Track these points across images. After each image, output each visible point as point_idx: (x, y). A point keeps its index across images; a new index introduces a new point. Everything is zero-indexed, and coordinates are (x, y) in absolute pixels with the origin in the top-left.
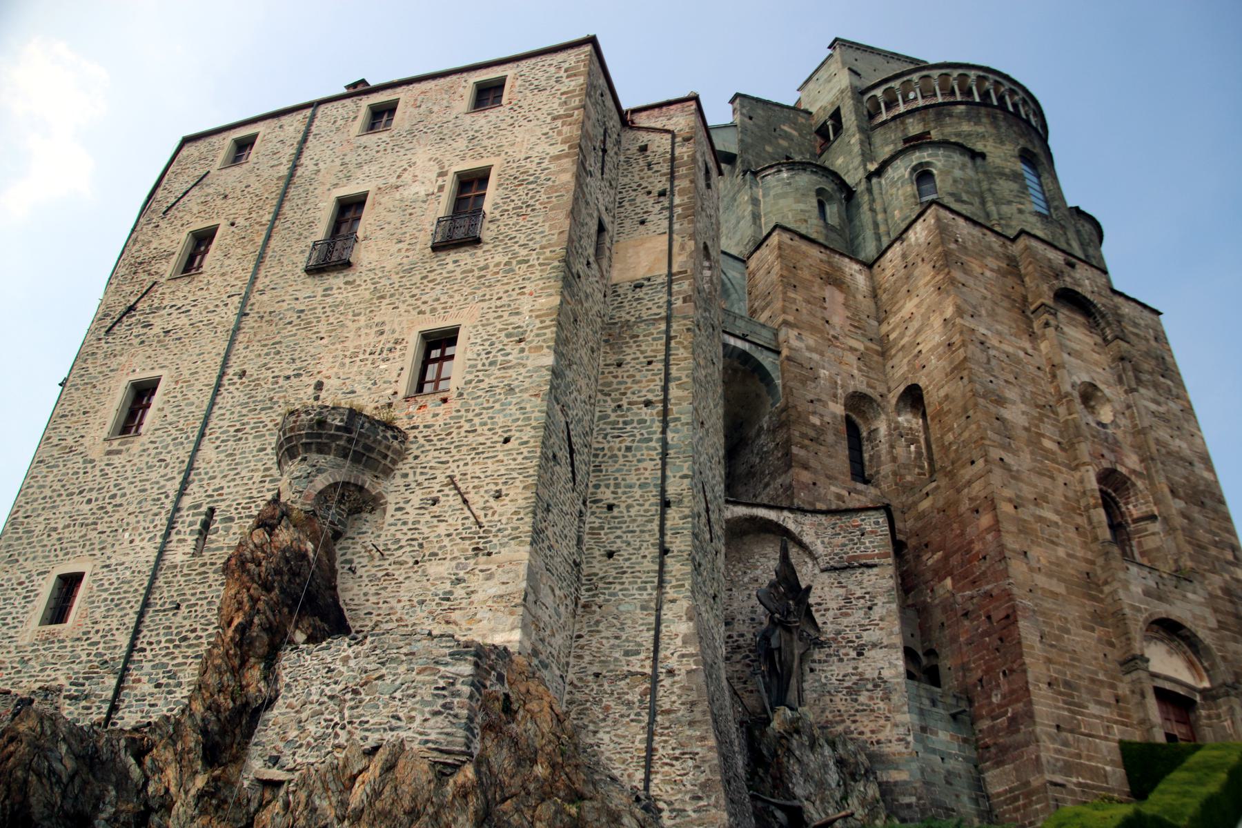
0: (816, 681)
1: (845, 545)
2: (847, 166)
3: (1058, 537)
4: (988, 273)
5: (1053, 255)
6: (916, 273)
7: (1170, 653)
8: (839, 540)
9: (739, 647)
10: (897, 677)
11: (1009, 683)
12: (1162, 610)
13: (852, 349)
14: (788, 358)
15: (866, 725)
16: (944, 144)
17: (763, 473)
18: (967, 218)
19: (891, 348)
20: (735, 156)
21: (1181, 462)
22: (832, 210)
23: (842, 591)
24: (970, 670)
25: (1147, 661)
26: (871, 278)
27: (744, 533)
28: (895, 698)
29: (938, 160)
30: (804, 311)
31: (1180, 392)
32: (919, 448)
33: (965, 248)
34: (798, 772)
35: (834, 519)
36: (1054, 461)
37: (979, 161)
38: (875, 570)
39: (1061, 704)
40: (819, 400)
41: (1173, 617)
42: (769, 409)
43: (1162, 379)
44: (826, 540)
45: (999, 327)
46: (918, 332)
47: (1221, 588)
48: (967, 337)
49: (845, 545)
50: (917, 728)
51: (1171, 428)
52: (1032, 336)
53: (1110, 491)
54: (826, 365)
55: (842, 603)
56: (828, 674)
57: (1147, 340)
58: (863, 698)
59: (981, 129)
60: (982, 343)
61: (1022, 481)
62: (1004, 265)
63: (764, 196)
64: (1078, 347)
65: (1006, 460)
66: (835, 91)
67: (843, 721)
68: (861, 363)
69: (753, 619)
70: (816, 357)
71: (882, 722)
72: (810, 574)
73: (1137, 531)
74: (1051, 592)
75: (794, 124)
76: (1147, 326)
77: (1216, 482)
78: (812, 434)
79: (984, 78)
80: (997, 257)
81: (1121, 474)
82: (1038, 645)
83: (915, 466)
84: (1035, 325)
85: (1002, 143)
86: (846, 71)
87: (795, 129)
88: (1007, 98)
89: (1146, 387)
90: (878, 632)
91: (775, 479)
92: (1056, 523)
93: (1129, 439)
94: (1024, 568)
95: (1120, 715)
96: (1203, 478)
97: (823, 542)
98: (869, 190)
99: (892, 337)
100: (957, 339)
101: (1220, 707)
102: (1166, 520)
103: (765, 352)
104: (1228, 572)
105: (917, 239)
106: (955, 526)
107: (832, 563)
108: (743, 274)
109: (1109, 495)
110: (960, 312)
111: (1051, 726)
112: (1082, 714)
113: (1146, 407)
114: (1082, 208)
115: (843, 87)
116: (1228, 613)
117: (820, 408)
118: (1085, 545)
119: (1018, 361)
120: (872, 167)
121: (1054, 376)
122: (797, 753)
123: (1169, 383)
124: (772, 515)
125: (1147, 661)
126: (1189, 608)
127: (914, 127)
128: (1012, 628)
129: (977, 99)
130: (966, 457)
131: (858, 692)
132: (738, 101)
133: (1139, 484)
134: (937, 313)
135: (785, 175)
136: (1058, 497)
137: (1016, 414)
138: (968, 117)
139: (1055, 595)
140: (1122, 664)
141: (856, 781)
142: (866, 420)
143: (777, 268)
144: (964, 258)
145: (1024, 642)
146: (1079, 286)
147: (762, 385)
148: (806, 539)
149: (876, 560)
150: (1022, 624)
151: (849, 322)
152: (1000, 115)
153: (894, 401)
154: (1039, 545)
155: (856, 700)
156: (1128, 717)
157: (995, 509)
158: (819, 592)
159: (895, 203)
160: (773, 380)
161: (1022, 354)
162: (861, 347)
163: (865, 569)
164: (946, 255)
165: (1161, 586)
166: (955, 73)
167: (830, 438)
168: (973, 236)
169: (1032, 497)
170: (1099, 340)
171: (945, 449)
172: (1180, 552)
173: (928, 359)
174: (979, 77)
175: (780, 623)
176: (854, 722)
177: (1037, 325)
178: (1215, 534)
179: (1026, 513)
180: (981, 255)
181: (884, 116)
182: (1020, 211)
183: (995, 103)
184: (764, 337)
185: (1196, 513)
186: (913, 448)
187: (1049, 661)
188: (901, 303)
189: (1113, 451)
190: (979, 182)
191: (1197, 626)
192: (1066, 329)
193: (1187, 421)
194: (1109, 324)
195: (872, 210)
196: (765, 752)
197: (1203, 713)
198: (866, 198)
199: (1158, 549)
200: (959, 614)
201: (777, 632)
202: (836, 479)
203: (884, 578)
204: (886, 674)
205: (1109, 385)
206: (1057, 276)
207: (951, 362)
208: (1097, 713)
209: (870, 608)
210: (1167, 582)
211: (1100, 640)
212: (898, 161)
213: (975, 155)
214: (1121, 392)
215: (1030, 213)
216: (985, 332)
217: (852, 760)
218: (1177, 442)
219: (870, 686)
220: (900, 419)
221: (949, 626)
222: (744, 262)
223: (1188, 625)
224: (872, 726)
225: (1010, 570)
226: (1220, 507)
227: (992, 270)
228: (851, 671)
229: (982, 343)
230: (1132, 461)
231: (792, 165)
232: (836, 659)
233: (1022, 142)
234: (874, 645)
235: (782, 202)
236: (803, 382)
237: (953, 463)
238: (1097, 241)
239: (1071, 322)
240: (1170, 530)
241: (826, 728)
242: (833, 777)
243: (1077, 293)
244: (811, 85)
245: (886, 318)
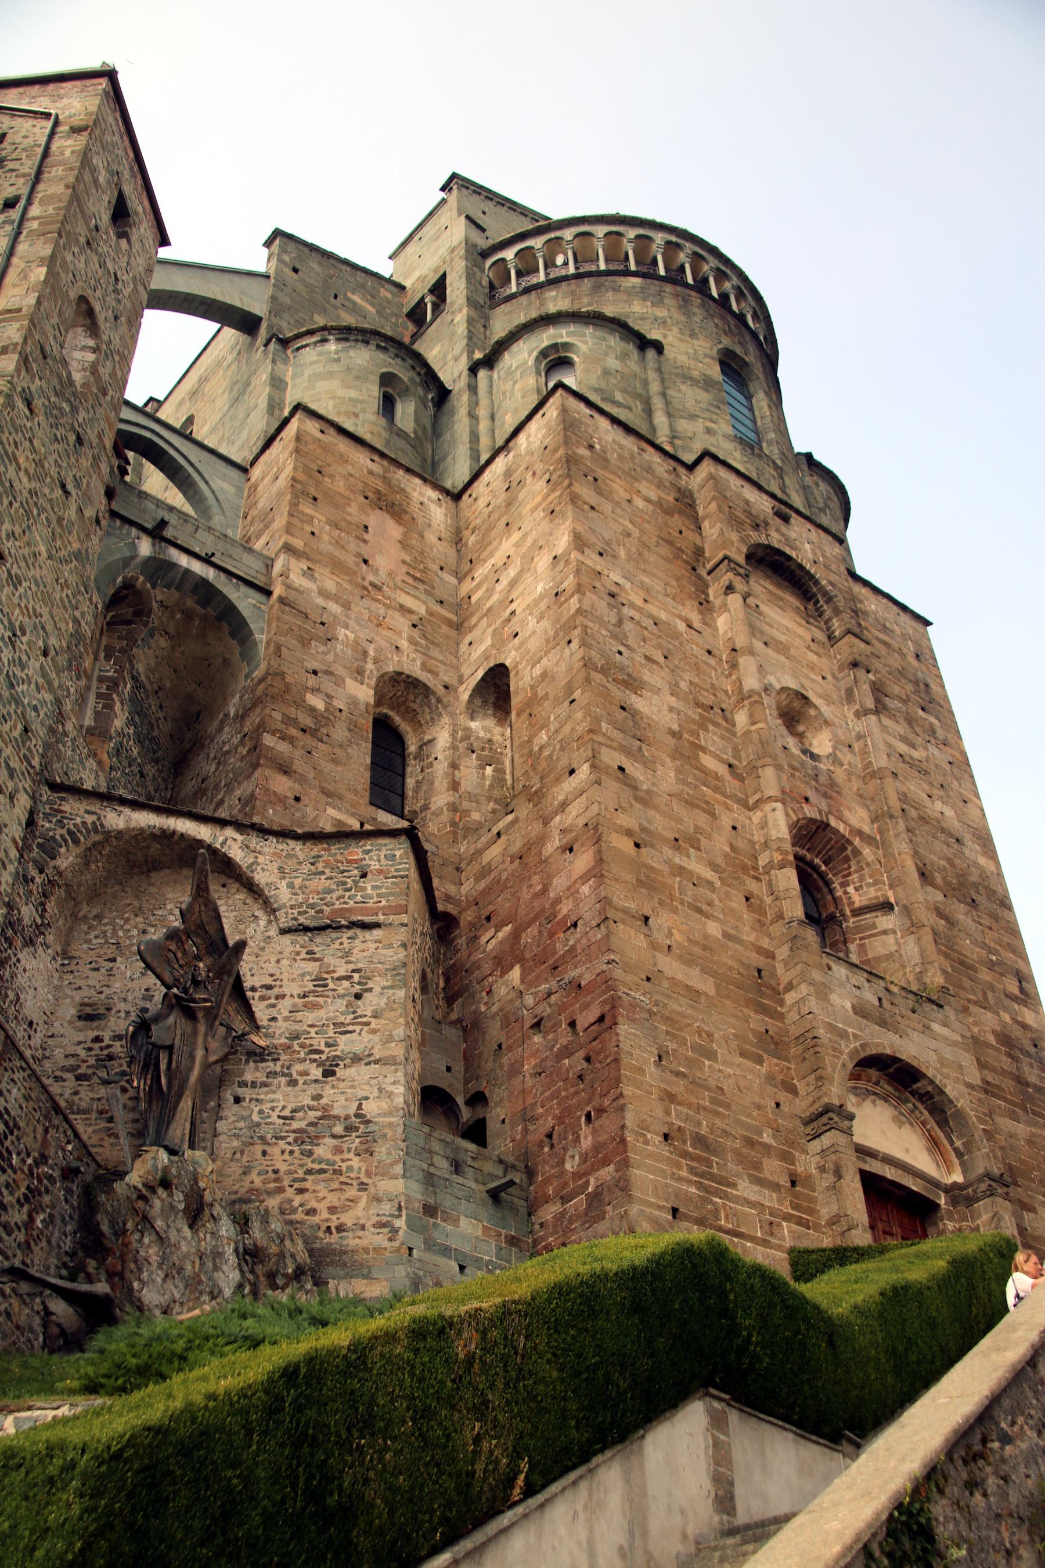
0: (243, 1118)
1: (330, 891)
2: (445, 355)
3: (710, 904)
4: (639, 503)
6: (521, 497)
7: (898, 1121)
8: (322, 883)
9: (110, 1058)
10: (390, 1114)
11: (595, 1132)
12: (886, 1042)
13: (403, 609)
14: (282, 600)
15: (322, 1197)
16: (596, 319)
17: (217, 787)
18: (615, 420)
19: (472, 614)
20: (259, 320)
21: (942, 837)
22: (406, 413)
23: (312, 967)
24: (534, 1119)
25: (851, 1117)
26: (457, 515)
27: (152, 866)
28: (382, 1150)
29: (584, 342)
30: (326, 537)
31: (949, 736)
32: (500, 771)
33: (606, 460)
34: (154, 1259)
35: (317, 849)
36: (716, 789)
37: (651, 354)
38: (377, 933)
39: (684, 1173)
40: (327, 672)
41: (904, 1057)
42: (242, 683)
43: (921, 712)
44: (298, 882)
45: (647, 580)
46: (513, 584)
47: (993, 1032)
48: (585, 580)
49: (330, 891)
50: (417, 1206)
51: (931, 784)
52: (704, 604)
53: (817, 861)
54: (352, 623)
55: (310, 986)
56: (266, 1107)
57: (903, 655)
58: (323, 1150)
59: (661, 313)
60: (612, 595)
61: (656, 808)
62: (671, 499)
63: (294, 376)
64: (783, 638)
65: (629, 770)
66: (443, 251)
67: (280, 1190)
68: (416, 633)
69: (145, 1010)
70: (334, 608)
71: (352, 1192)
72: (259, 936)
73: (859, 929)
74: (687, 986)
75: (372, 296)
76: (905, 636)
77: (1000, 874)
78: (308, 721)
79: (678, 245)
80: (660, 484)
81: (836, 831)
82: (651, 1069)
83: (490, 799)
84: (711, 592)
85: (693, 335)
86: (463, 218)
87: (372, 305)
88: (712, 280)
89: (892, 717)
90: (366, 1037)
91: (233, 791)
92: (710, 883)
93: (856, 784)
94: (641, 941)
95: (796, 1207)
96: (976, 865)
97: (291, 886)
98: (473, 389)
99: (474, 599)
100: (569, 583)
101: (980, 1216)
102: (907, 910)
103: (244, 589)
104: (1006, 1009)
105: (529, 443)
106: (536, 879)
107: (302, 920)
108: (240, 489)
109: (816, 868)
110: (579, 542)
111: (660, 1208)
112: (725, 1196)
113: (890, 746)
114: (817, 457)
115: (455, 243)
116: (1004, 1072)
117: (327, 684)
118: (761, 925)
119: (676, 635)
120: (478, 355)
121: (734, 666)
122: (159, 1223)
123: (933, 720)
124: (203, 832)
125: (851, 1117)
126: (931, 1046)
127: (556, 301)
128: (606, 1035)
129: (662, 272)
130: (563, 763)
131: (315, 1140)
132: (277, 242)
133: (867, 852)
134: (545, 551)
135: (332, 346)
136: (720, 843)
137: (658, 707)
138: (643, 295)
139: (694, 994)
140: (806, 1123)
141: (274, 1287)
142: (418, 726)
143: (289, 470)
144: (600, 473)
145: (625, 1059)
146: (792, 548)
147: (233, 643)
148: (261, 878)
149: (381, 918)
150: (623, 1028)
151: (405, 569)
152: (696, 298)
153: (465, 695)
154: (675, 910)
155: (310, 1153)
156: (811, 1211)
157: (598, 841)
158: (271, 968)
159: (508, 404)
160: (251, 633)
161: (682, 626)
162: (422, 610)
163: (358, 931)
164: (570, 461)
165: (886, 1004)
166: (632, 233)
167: (340, 732)
168: (621, 447)
169: (672, 836)
170: (821, 636)
171: (533, 757)
172: (925, 962)
173: (524, 622)
174: (669, 243)
175: (181, 1005)
176: (301, 1191)
177: (714, 592)
178: (990, 951)
179: (655, 858)
180: (632, 476)
181: (514, 288)
182: (709, 431)
183: (690, 280)
184: (248, 566)
185: (960, 912)
186: (489, 770)
187: (670, 1097)
188: (495, 543)
189: (825, 795)
190: (646, 383)
191: (947, 1077)
192: (763, 608)
193: (958, 780)
194: (837, 611)
195: (473, 416)
196: (105, 1228)
197: (950, 1225)
198: (465, 398)
199: (890, 957)
200: (527, 1025)
201: (171, 1019)
202: (340, 797)
203: (390, 946)
204: (370, 1108)
205: (829, 702)
206: (756, 527)
207: (557, 620)
208: (753, 1198)
209: (358, 996)
210: (899, 1000)
211: (770, 1078)
212: (521, 342)
213: (644, 343)
214: (850, 715)
215: (726, 436)
216: (621, 581)
217: (274, 1249)
218: (938, 806)
219: (339, 1129)
220: (474, 725)
221: (510, 1049)
222: (245, 470)
223: (930, 1073)
224: (333, 1199)
225: (613, 939)
226: (1002, 912)
227: (647, 500)
228: (307, 1101)
229: (612, 595)
230: (852, 818)
231: (346, 333)
232: (283, 1080)
233: (726, 342)
234: (356, 1059)
235: (322, 386)
236: (305, 642)
237: (542, 778)
238: (839, 513)
239: (774, 600)
240: (914, 927)
241: (248, 1201)
242: (229, 1276)
243: (789, 558)
244: (410, 249)
245: (471, 570)
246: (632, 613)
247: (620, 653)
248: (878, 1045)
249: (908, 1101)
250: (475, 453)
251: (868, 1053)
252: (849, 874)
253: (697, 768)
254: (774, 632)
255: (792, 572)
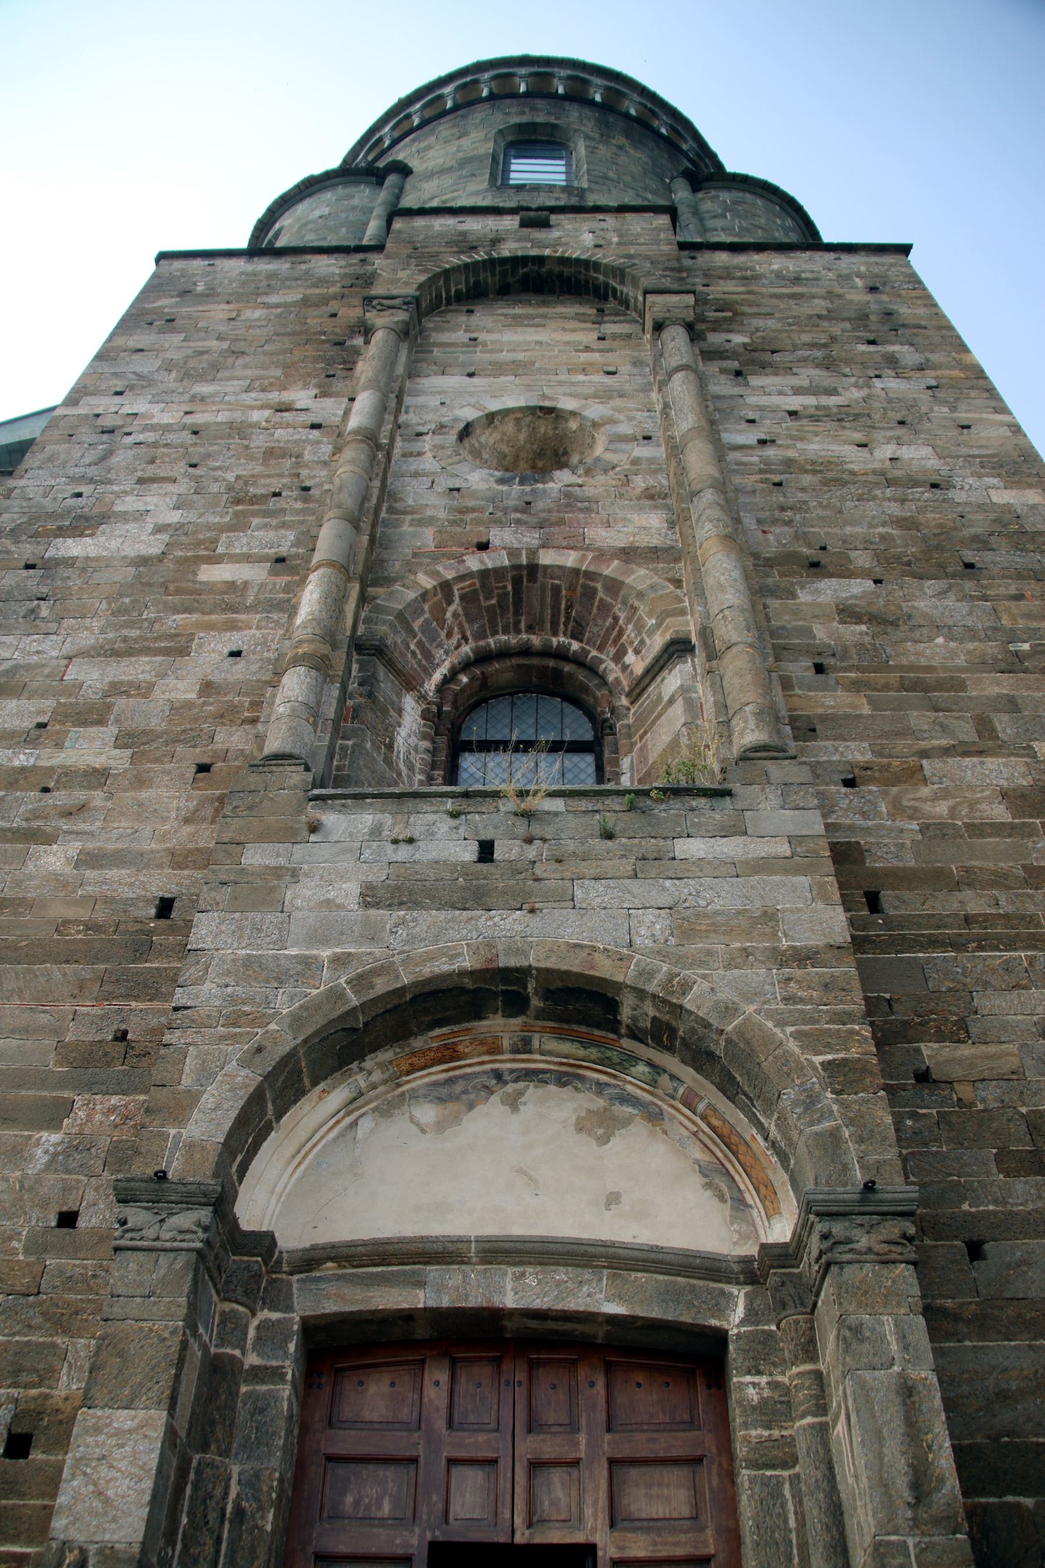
4: (258, 313)
5: (474, 225)
12: (448, 943)
37: (391, 179)
43: (863, 348)
64: (520, 356)
76: (844, 278)
109: (562, 654)
133: (639, 577)
233: (515, 120)
243: (540, 260)
246: (141, 438)
247: (79, 495)
248: (431, 957)
249: (633, 1059)
251: (382, 986)
252: (621, 634)
253: (178, 592)
254: (505, 356)
255: (560, 275)
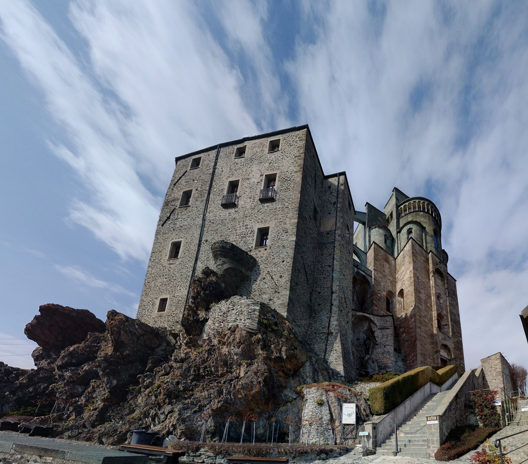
8: (382, 322)
15: (385, 360)
42: (369, 292)
46: (404, 275)
59: (426, 220)
70: (381, 280)
127: (410, 219)
137: (423, 296)
138: (423, 216)
148: (375, 322)
175: (368, 338)
179: (421, 319)
187: (422, 350)
242: (377, 369)
250: (398, 251)
